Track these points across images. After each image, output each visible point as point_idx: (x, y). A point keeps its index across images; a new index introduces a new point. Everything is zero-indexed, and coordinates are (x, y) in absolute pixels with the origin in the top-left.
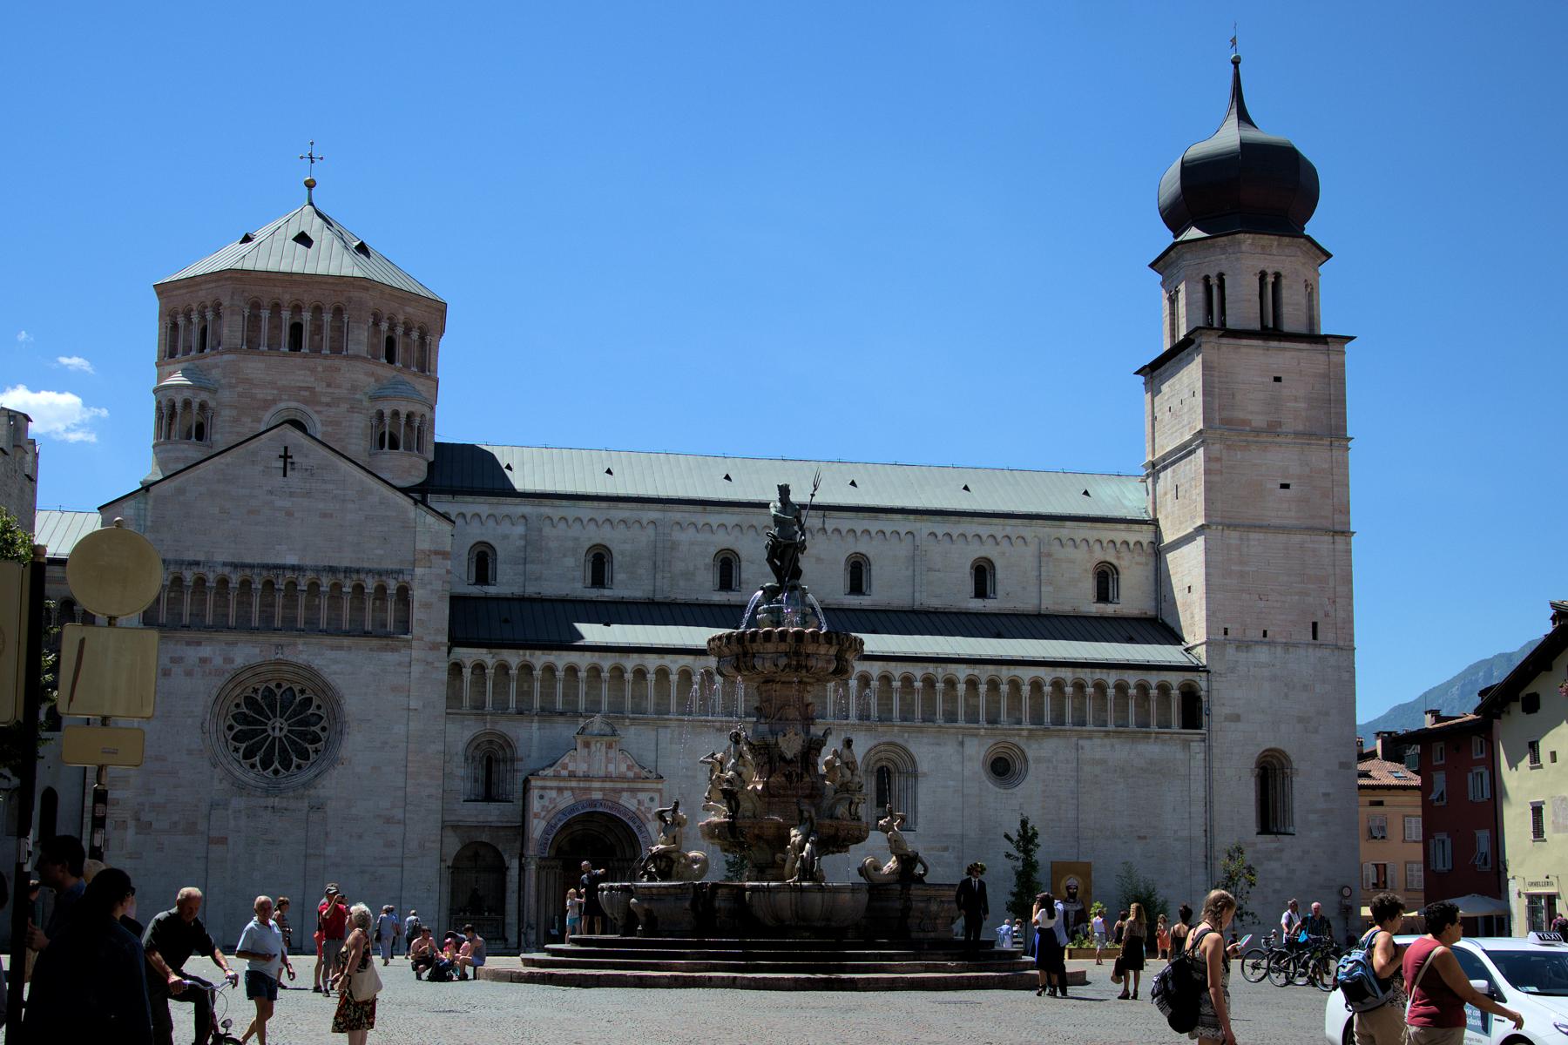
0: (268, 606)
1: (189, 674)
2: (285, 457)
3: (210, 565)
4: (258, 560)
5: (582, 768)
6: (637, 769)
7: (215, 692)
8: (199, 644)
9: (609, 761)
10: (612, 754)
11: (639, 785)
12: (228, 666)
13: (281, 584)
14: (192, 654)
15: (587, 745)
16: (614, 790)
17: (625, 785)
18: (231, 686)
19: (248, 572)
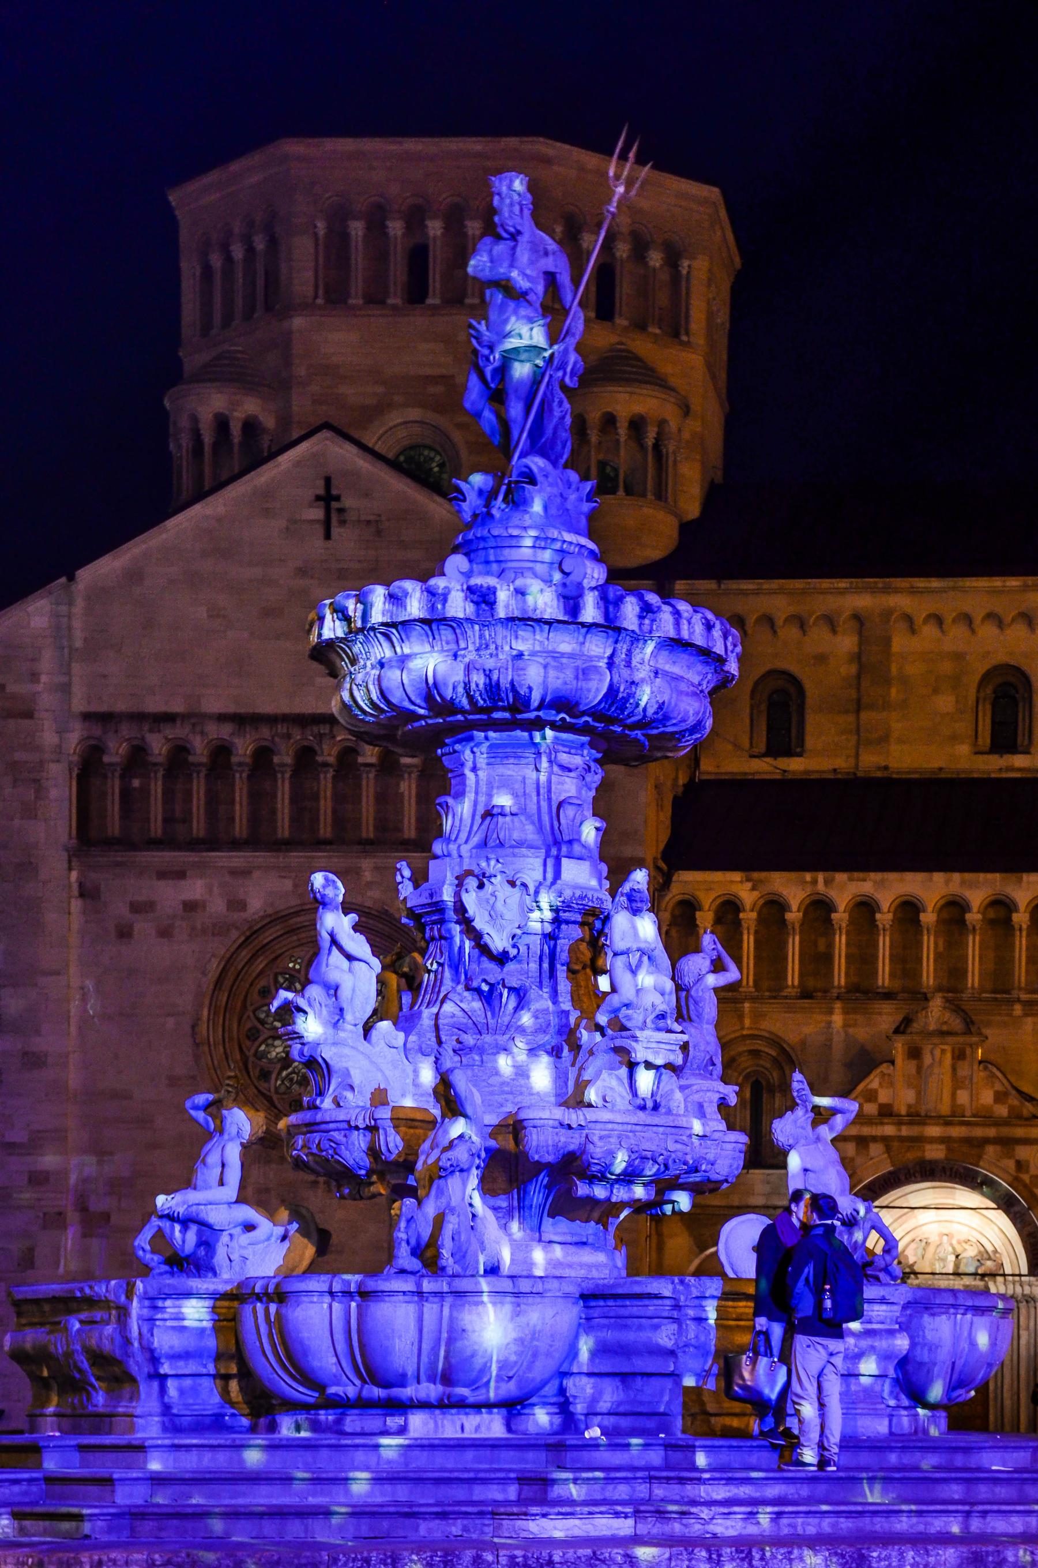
0: (303, 803)
1: (165, 933)
2: (327, 498)
3: (195, 718)
4: (284, 706)
5: (904, 1098)
6: (1014, 1101)
7: (214, 967)
8: (180, 875)
9: (957, 1083)
10: (964, 1070)
11: (1019, 1132)
12: (236, 916)
13: (328, 754)
14: (170, 896)
15: (914, 1053)
16: (968, 1141)
17: (991, 1132)
18: (245, 954)
19: (265, 732)
